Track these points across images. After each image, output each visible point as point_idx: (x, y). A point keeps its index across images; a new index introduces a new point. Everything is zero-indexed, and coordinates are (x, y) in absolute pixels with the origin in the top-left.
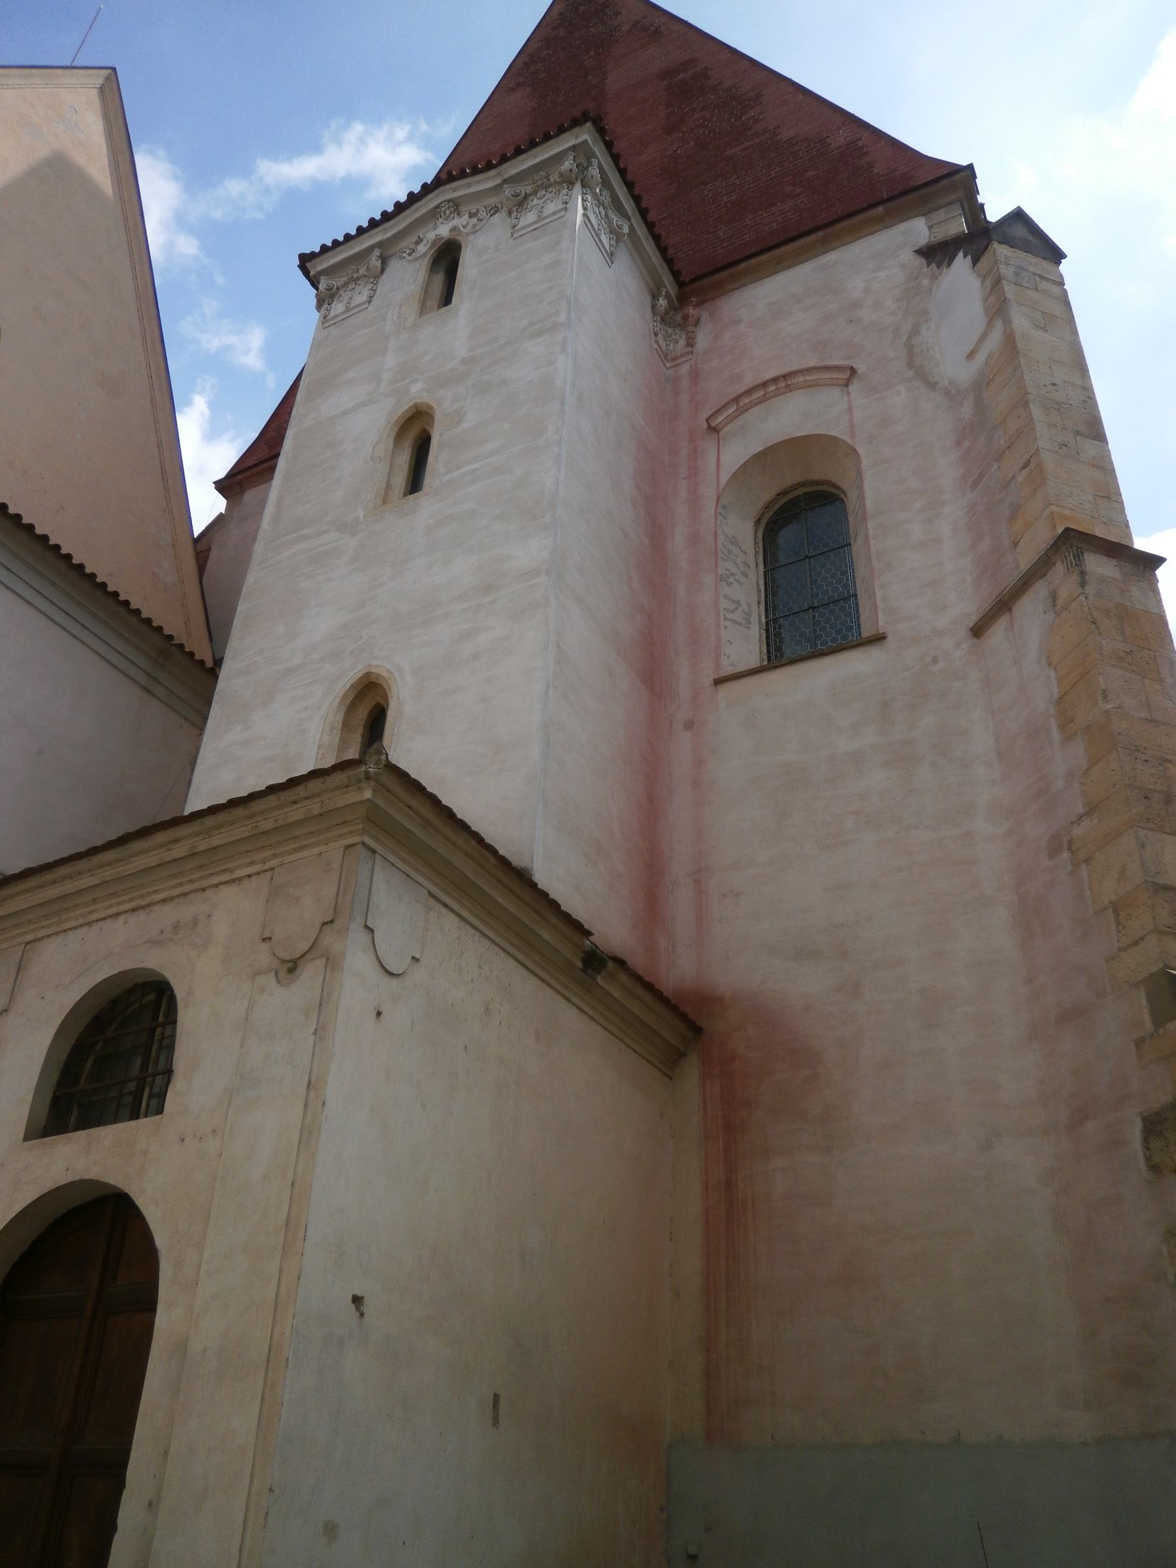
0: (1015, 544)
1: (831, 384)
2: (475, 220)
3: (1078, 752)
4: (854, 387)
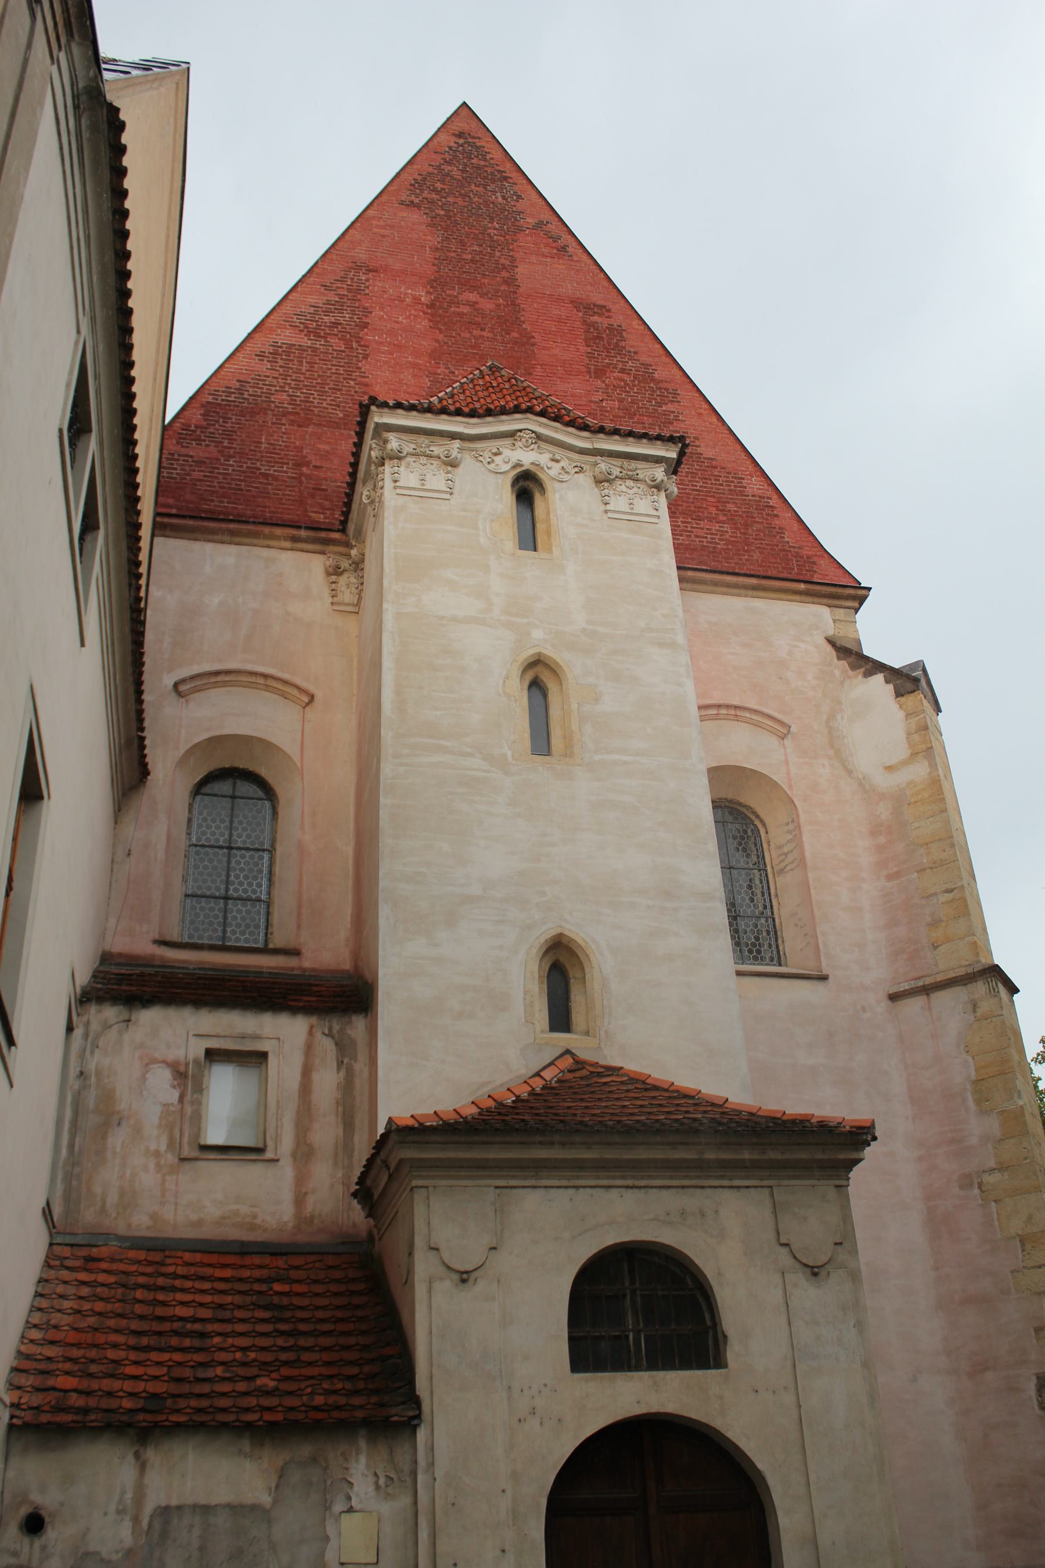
0: (935, 948)
1: (772, 731)
2: (558, 466)
3: (993, 1125)
4: (788, 742)
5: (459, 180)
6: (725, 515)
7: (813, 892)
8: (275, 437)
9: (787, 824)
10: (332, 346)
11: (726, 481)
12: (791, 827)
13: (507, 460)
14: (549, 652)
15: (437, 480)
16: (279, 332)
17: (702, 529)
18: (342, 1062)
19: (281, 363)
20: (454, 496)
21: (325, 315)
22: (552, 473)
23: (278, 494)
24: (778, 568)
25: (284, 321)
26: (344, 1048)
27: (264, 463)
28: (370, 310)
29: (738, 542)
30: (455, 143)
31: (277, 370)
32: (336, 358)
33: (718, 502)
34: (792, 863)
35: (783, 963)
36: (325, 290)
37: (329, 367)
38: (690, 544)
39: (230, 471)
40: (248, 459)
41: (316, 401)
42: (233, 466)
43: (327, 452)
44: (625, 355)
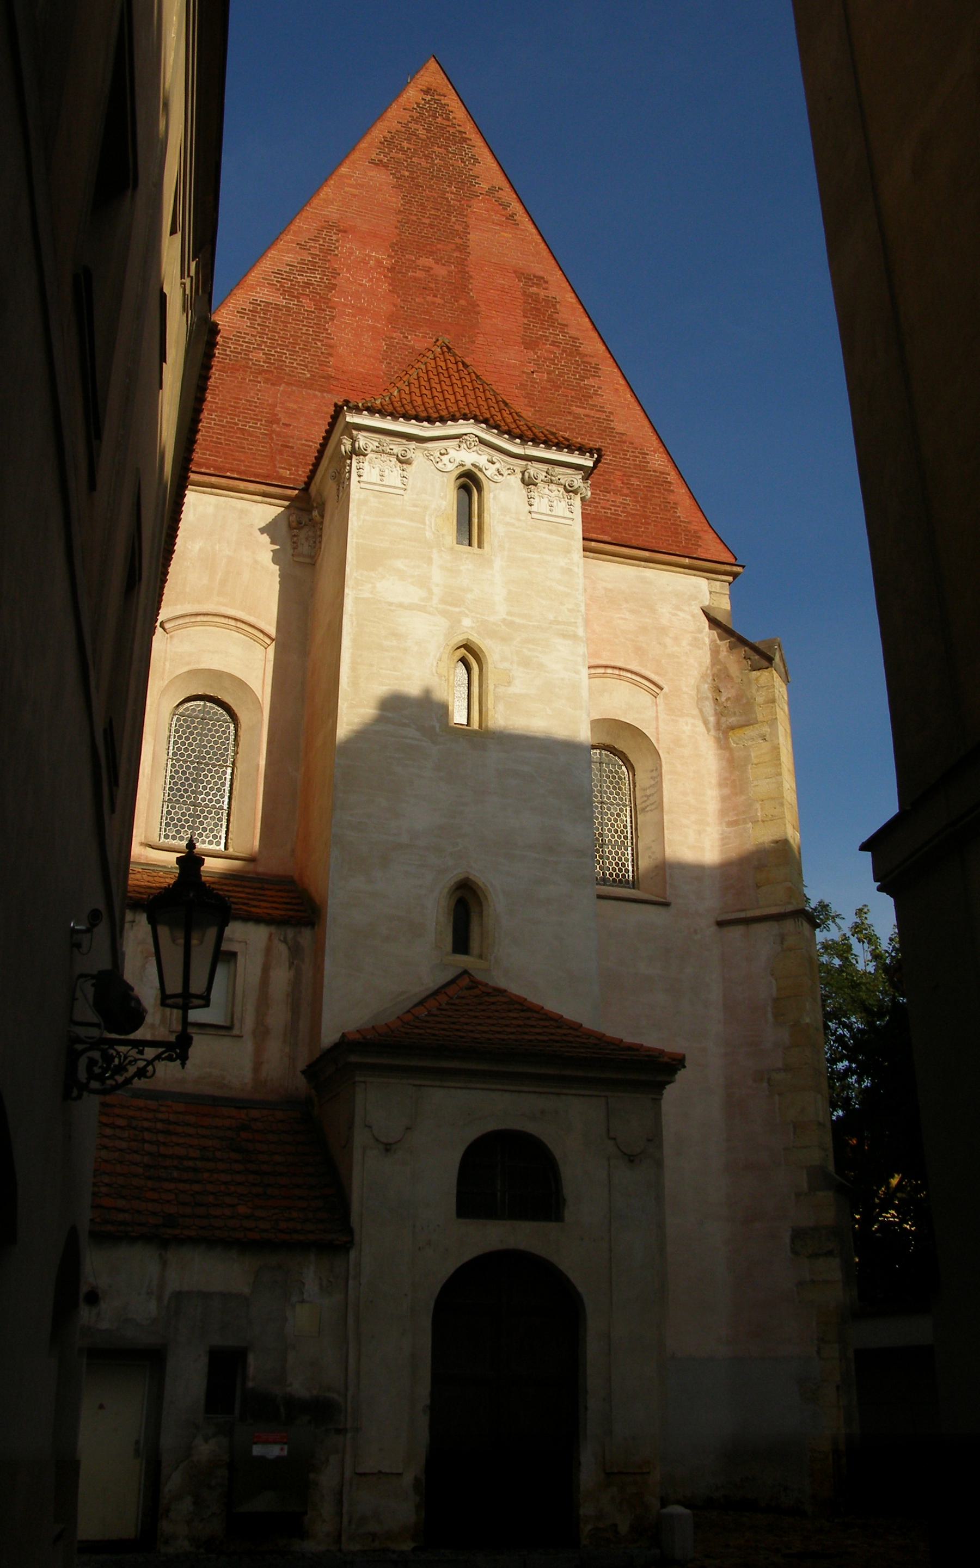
0: (758, 887)
4: (660, 700)
5: (424, 140)
6: (629, 488)
7: (666, 831)
8: (252, 394)
9: (652, 771)
10: (304, 306)
11: (632, 456)
12: (654, 774)
13: (452, 460)
14: (476, 639)
15: (394, 474)
16: (258, 290)
17: (608, 501)
18: (293, 963)
19: (259, 321)
20: (408, 491)
21: (298, 275)
22: (488, 473)
23: (252, 449)
24: (668, 540)
25: (263, 278)
26: (295, 951)
27: (241, 418)
28: (338, 271)
29: (637, 515)
30: (423, 99)
31: (255, 328)
32: (306, 318)
33: (624, 475)
34: (651, 804)
35: (636, 886)
36: (300, 248)
37: (300, 327)
38: (596, 515)
39: (212, 425)
40: (228, 414)
41: (288, 361)
42: (215, 420)
43: (295, 410)
44: (557, 327)
